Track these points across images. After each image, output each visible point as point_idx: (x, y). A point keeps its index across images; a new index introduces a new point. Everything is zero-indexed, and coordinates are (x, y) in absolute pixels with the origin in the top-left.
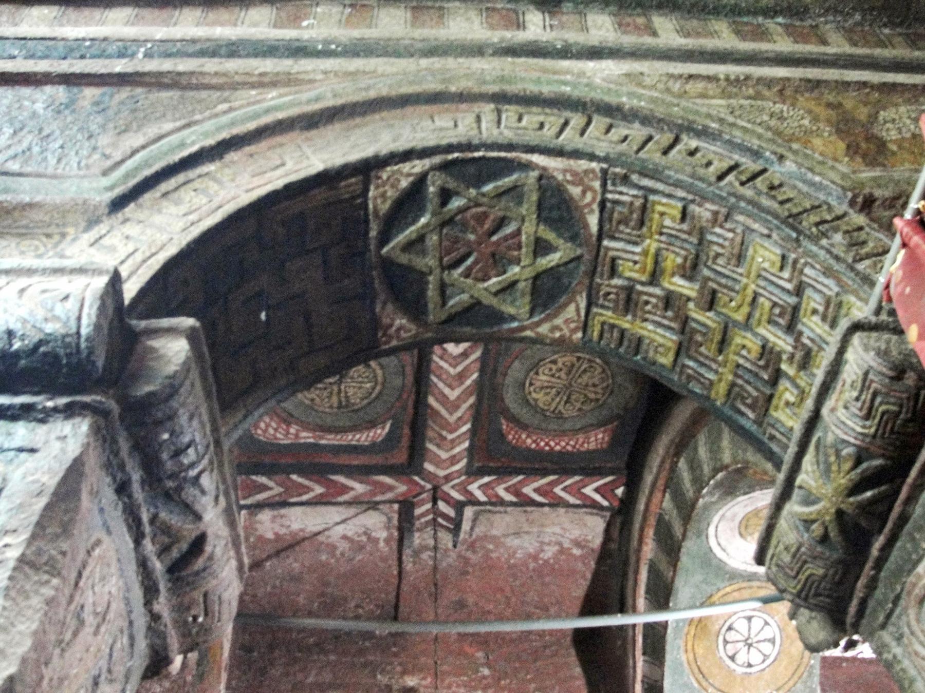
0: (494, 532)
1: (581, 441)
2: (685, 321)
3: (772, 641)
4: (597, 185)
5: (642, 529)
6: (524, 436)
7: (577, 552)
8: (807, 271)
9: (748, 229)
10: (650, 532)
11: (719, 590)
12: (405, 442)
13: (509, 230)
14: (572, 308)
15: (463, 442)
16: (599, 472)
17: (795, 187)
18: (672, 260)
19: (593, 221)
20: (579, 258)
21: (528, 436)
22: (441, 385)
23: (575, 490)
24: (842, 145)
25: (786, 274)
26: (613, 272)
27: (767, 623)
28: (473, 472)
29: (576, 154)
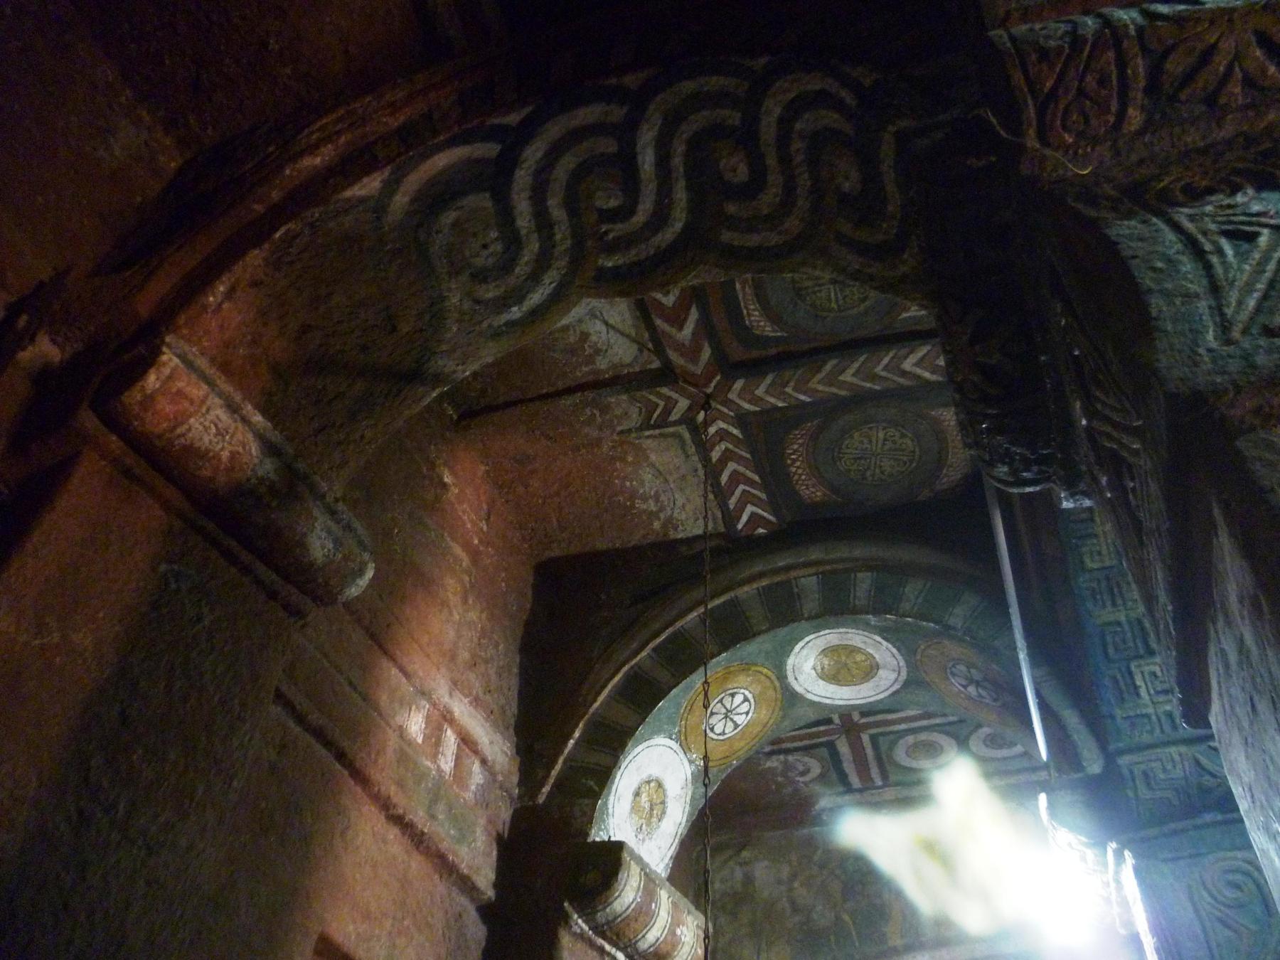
0: (653, 457)
1: (810, 483)
3: (736, 726)
5: (761, 575)
6: (800, 441)
10: (765, 582)
11: (762, 665)
12: (755, 354)
15: (784, 400)
16: (774, 506)
21: (801, 445)
22: (856, 365)
27: (747, 713)
28: (742, 420)
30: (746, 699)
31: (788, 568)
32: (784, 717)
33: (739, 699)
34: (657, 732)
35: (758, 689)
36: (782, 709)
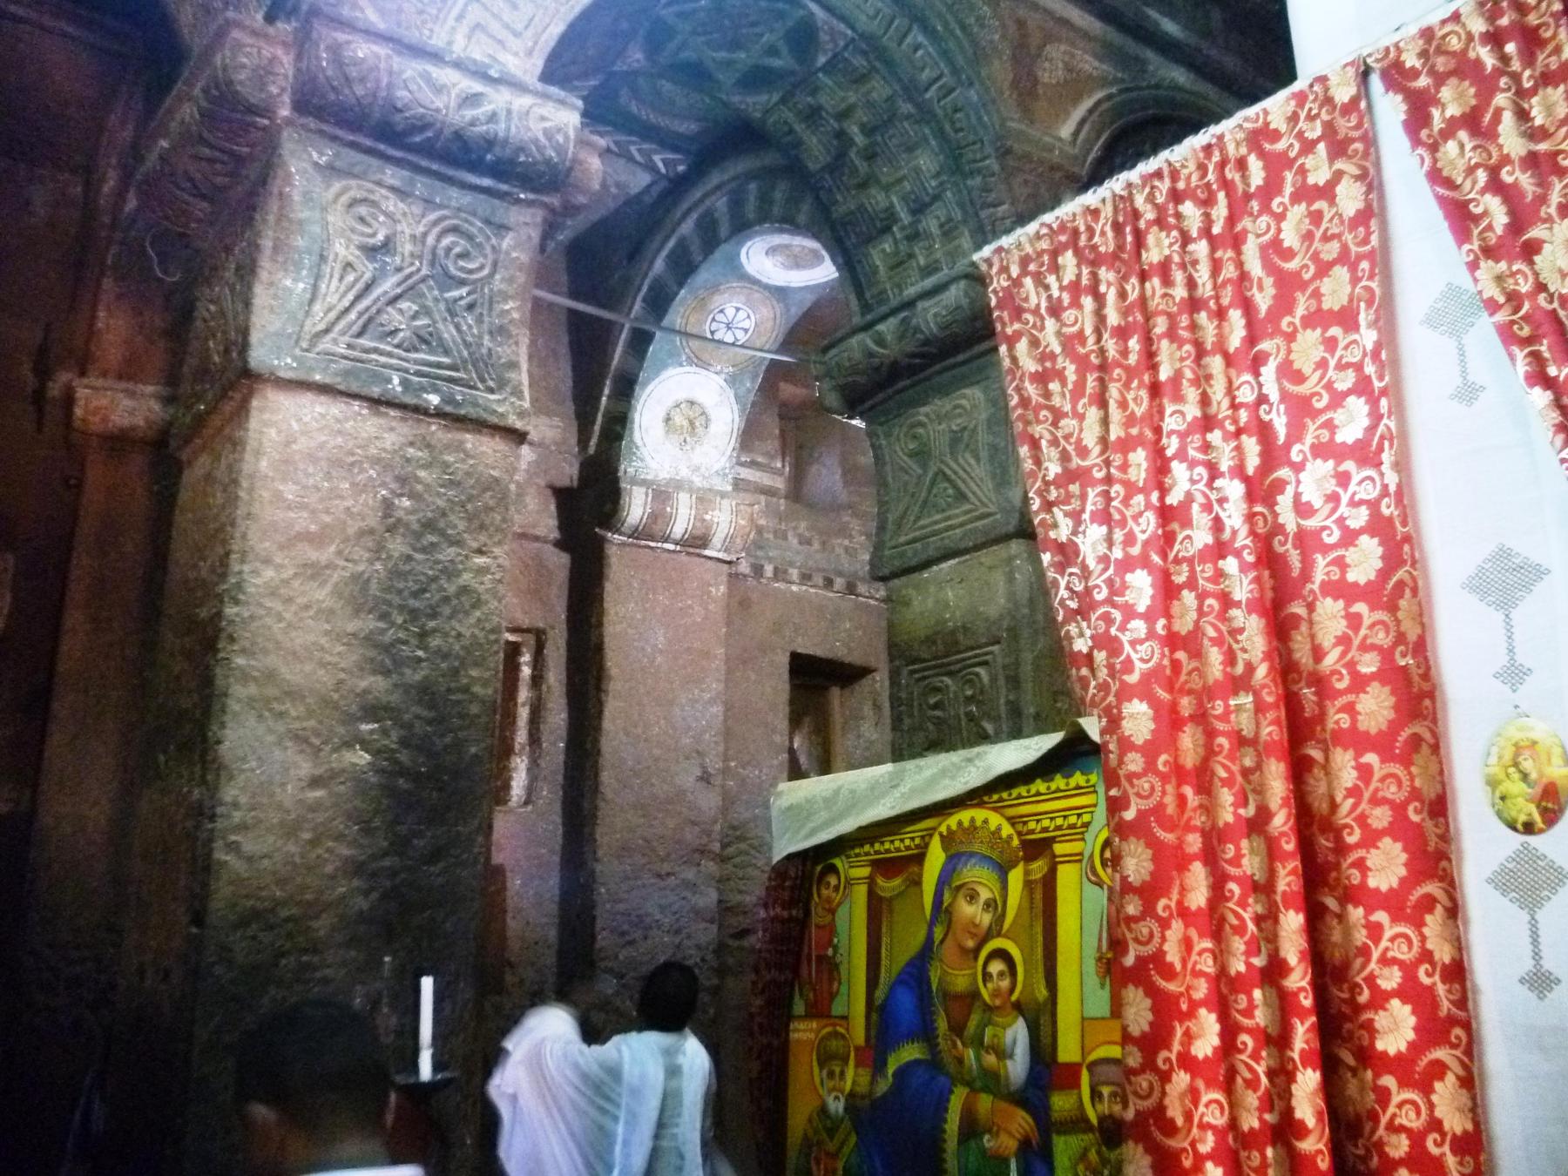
3: (746, 331)
4: (842, 43)
7: (613, 190)
8: (949, 194)
9: (926, 139)
10: (695, 216)
13: (757, 30)
14: (765, 97)
16: (675, 149)
17: (968, 116)
18: (861, 115)
19: (822, 60)
20: (793, 73)
23: (647, 154)
24: (1011, 76)
25: (934, 183)
26: (814, 92)
29: (842, 18)
30: (738, 309)
31: (701, 200)
33: (730, 312)
34: (665, 366)
35: (743, 298)
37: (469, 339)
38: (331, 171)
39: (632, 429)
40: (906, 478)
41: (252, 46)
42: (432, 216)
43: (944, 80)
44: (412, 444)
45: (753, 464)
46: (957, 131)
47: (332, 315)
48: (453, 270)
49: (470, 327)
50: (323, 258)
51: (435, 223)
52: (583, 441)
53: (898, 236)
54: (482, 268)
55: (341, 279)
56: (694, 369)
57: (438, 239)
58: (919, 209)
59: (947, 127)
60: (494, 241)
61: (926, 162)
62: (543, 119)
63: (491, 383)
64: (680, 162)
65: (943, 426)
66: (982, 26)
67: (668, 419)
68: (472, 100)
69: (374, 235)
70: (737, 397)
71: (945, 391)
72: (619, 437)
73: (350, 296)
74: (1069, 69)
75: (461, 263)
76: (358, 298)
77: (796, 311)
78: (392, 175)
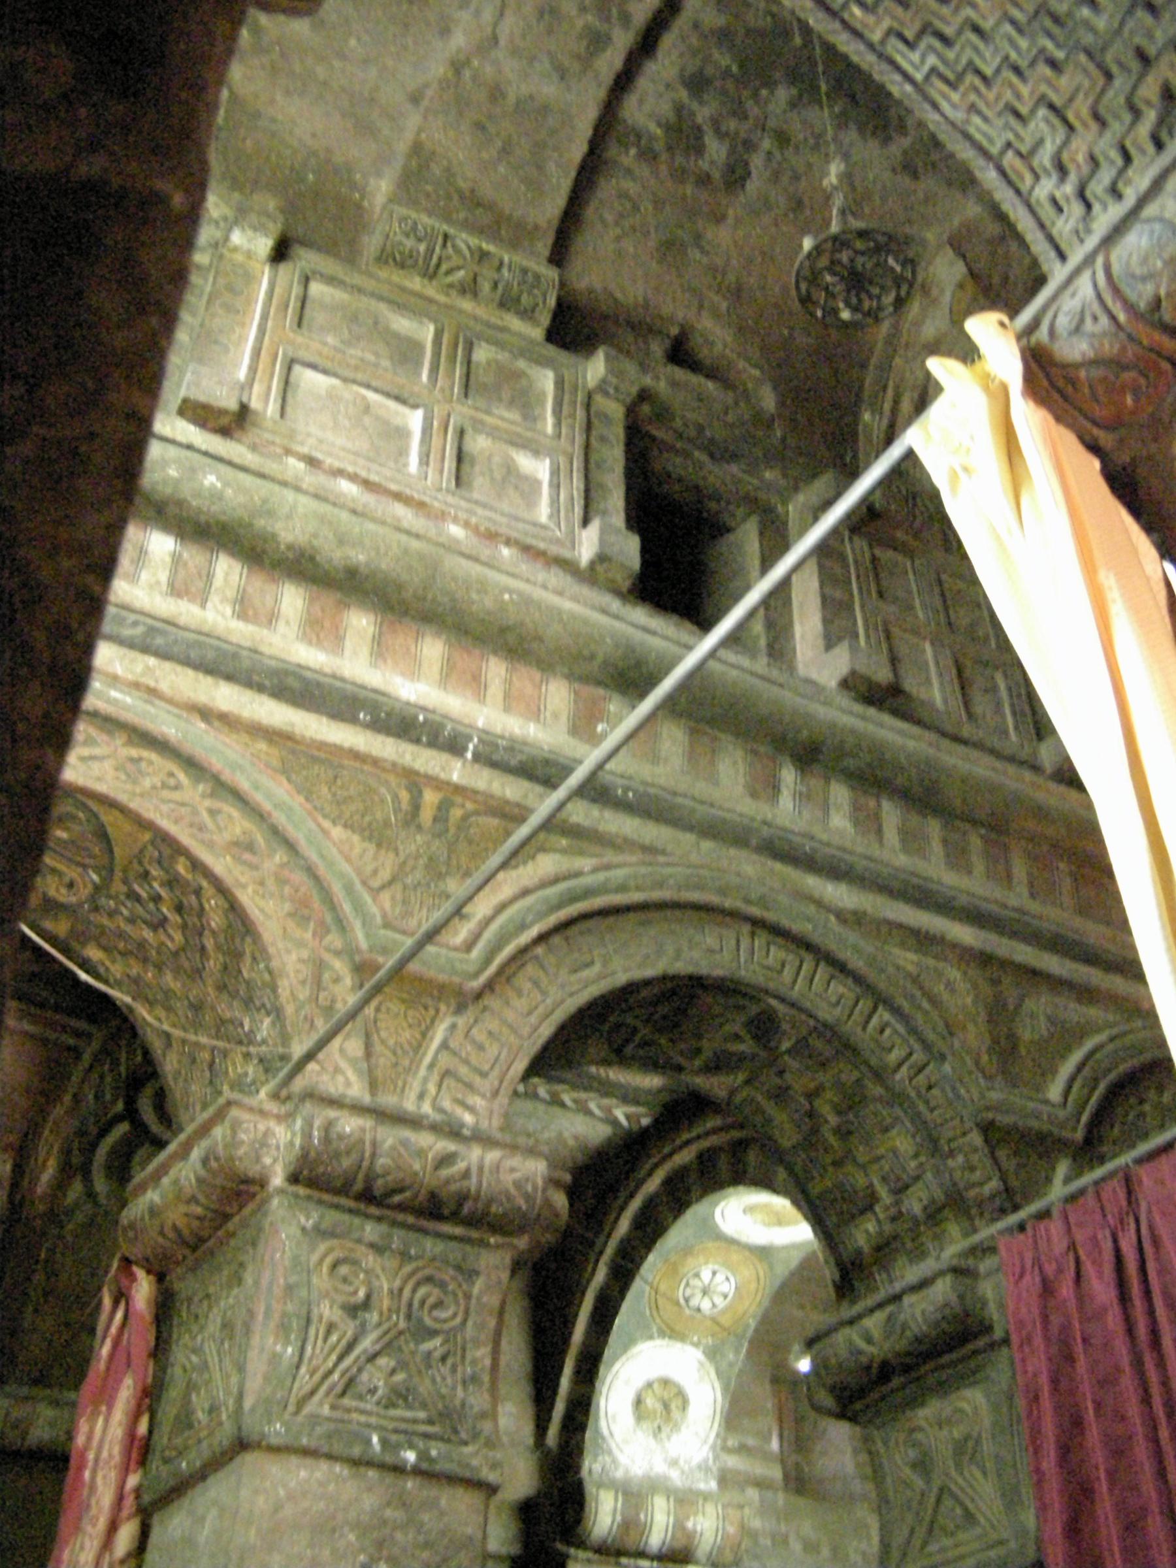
2: (815, 1131)
16: (637, 1103)
17: (943, 1090)
18: (829, 1095)
19: (786, 1045)
25: (913, 1164)
26: (781, 1073)
32: (771, 1268)
33: (706, 1275)
36: (761, 1261)
37: (444, 1391)
38: (320, 1233)
39: (597, 1420)
40: (909, 1493)
41: (249, 1121)
42: (408, 1269)
43: (915, 1057)
44: (389, 1504)
45: (742, 1449)
46: (932, 1110)
47: (318, 1376)
48: (428, 1321)
49: (444, 1379)
50: (308, 1321)
51: (413, 1273)
52: (541, 1427)
53: (881, 1216)
54: (455, 1315)
55: (325, 1339)
56: (666, 1342)
57: (414, 1291)
58: (900, 1190)
59: (922, 1107)
60: (465, 1286)
61: (902, 1142)
62: (512, 1170)
63: (464, 1435)
64: (645, 1116)
65: (945, 1432)
66: (953, 991)
67: (638, 1402)
68: (446, 1160)
69: (355, 1293)
70: (719, 1373)
71: (943, 1389)
72: (582, 1428)
73: (334, 1357)
74: (1052, 1020)
75: (435, 1313)
76: (341, 1358)
77: (782, 1270)
78: (371, 1231)
